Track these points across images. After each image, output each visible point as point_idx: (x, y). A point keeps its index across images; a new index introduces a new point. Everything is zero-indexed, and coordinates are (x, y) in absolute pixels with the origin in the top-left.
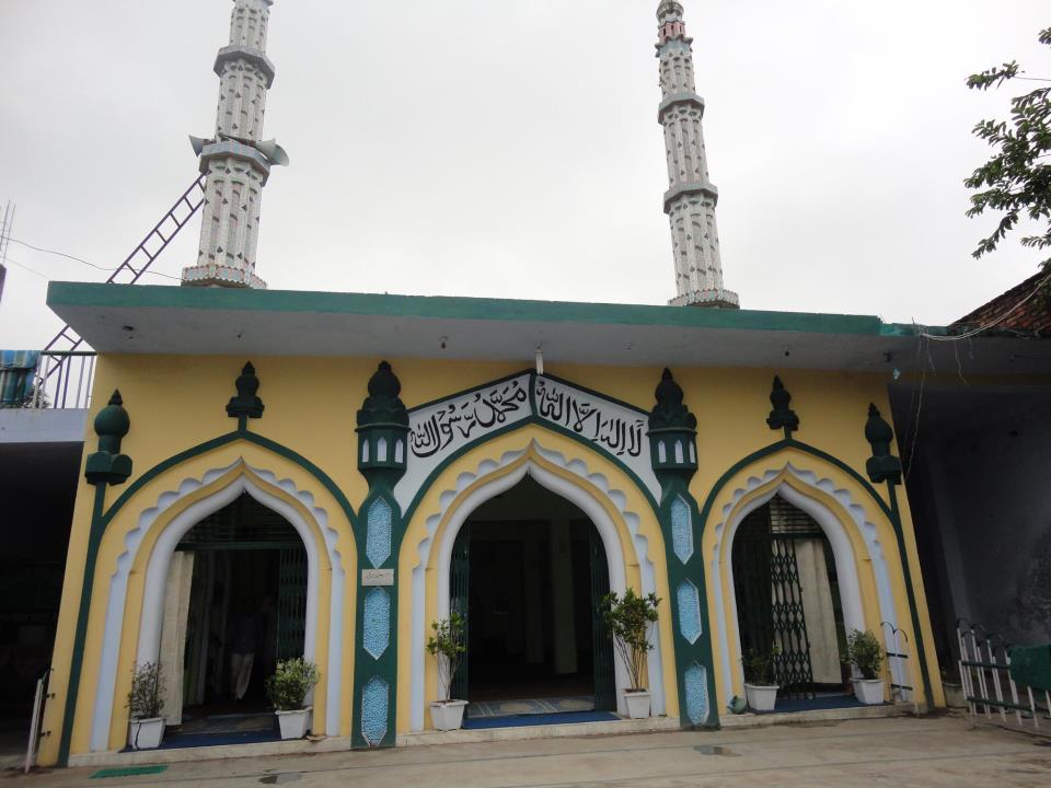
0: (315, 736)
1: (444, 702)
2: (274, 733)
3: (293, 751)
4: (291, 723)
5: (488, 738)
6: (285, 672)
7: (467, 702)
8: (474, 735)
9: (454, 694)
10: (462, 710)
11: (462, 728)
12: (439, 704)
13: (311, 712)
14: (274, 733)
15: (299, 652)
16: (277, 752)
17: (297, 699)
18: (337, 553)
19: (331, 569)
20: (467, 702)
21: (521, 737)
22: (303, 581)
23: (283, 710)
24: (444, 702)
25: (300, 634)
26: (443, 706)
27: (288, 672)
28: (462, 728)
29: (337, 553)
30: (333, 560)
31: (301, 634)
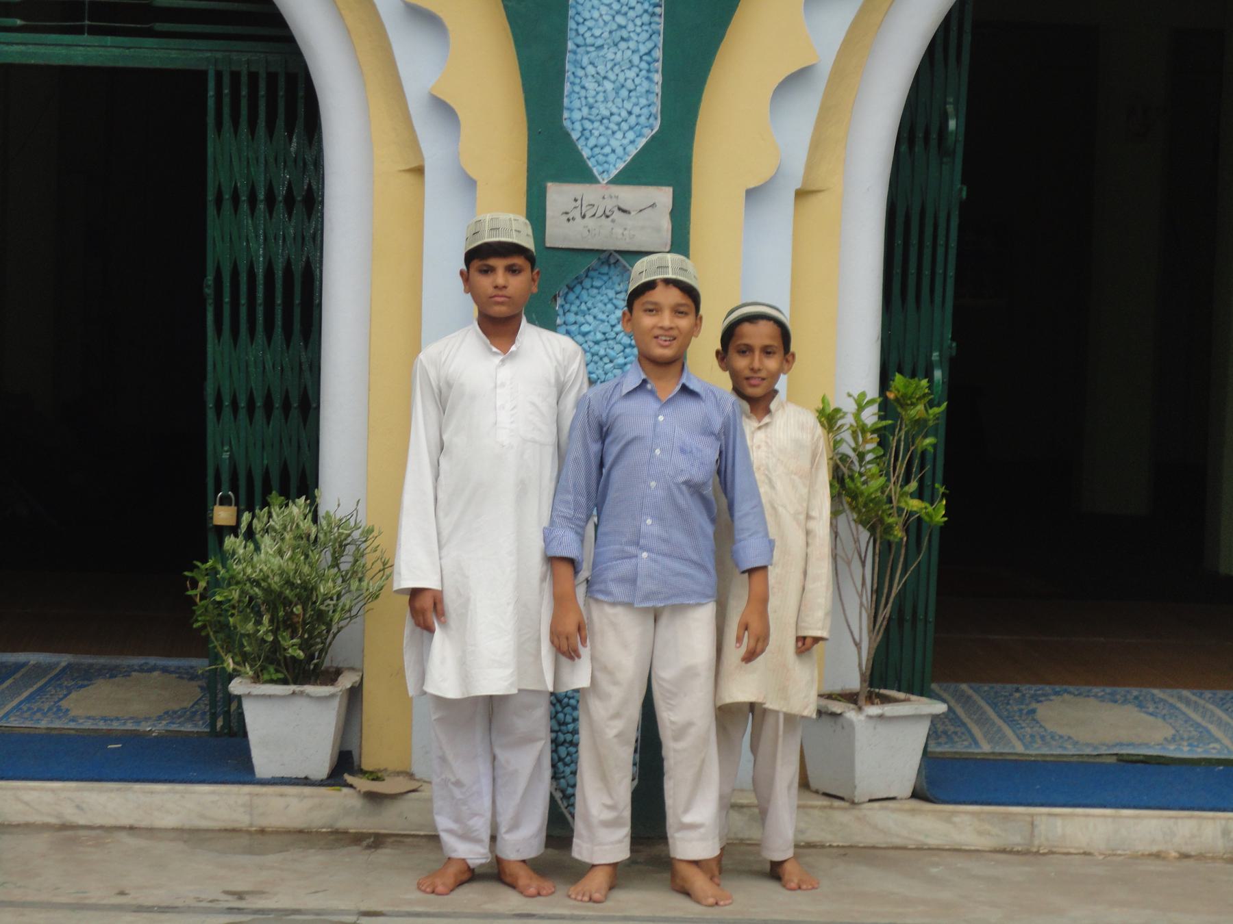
0: (375, 776)
1: (851, 698)
2: (220, 751)
3: (299, 823)
4: (286, 726)
5: (1015, 839)
6: (260, 550)
7: (940, 708)
8: (963, 825)
9: (888, 674)
10: (920, 732)
11: (916, 795)
12: (836, 707)
13: (355, 695)
14: (220, 751)
15: (301, 480)
16: (242, 819)
17: (305, 645)
18: (444, 109)
19: (419, 171)
20: (940, 708)
21: (1143, 847)
22: (307, 202)
23: (257, 679)
24: (851, 698)
25: (301, 406)
26: (851, 714)
27: (267, 542)
28: (916, 795)
29: (444, 109)
30: (434, 148)
31: (305, 406)
